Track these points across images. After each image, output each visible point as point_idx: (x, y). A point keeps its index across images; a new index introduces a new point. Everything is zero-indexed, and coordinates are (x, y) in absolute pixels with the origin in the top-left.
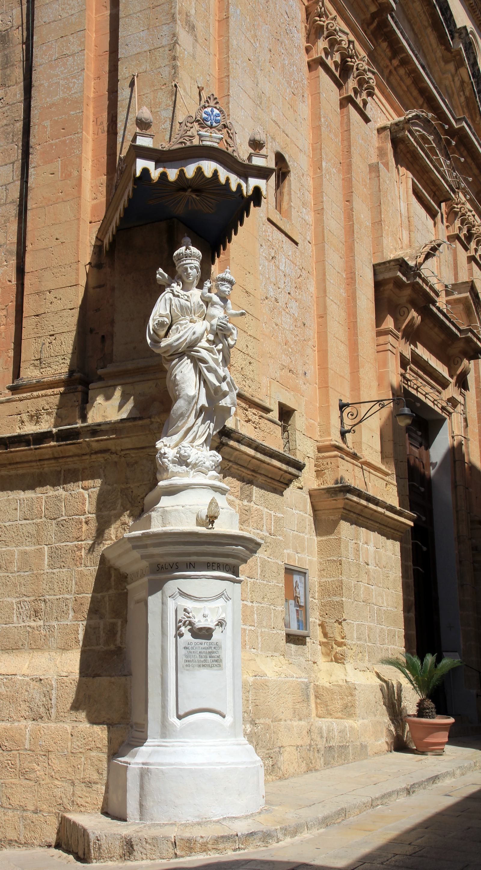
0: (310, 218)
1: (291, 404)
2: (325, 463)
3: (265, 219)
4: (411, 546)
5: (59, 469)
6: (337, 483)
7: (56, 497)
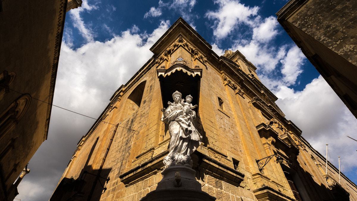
1: (237, 158)
2: (256, 180)
6: (262, 186)
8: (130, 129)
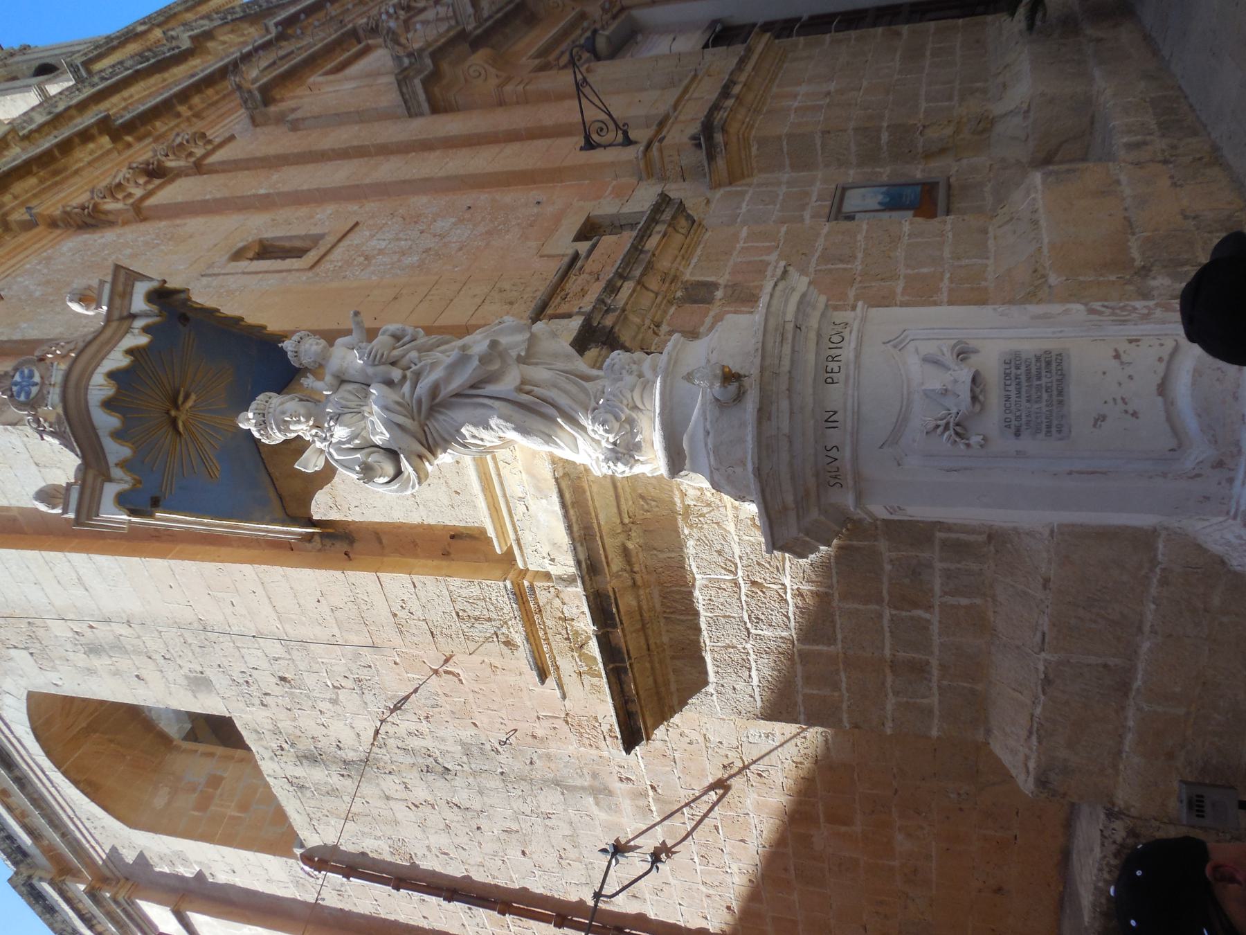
0: (330, 209)
3: (310, 274)
4: (802, 39)
8: (361, 767)
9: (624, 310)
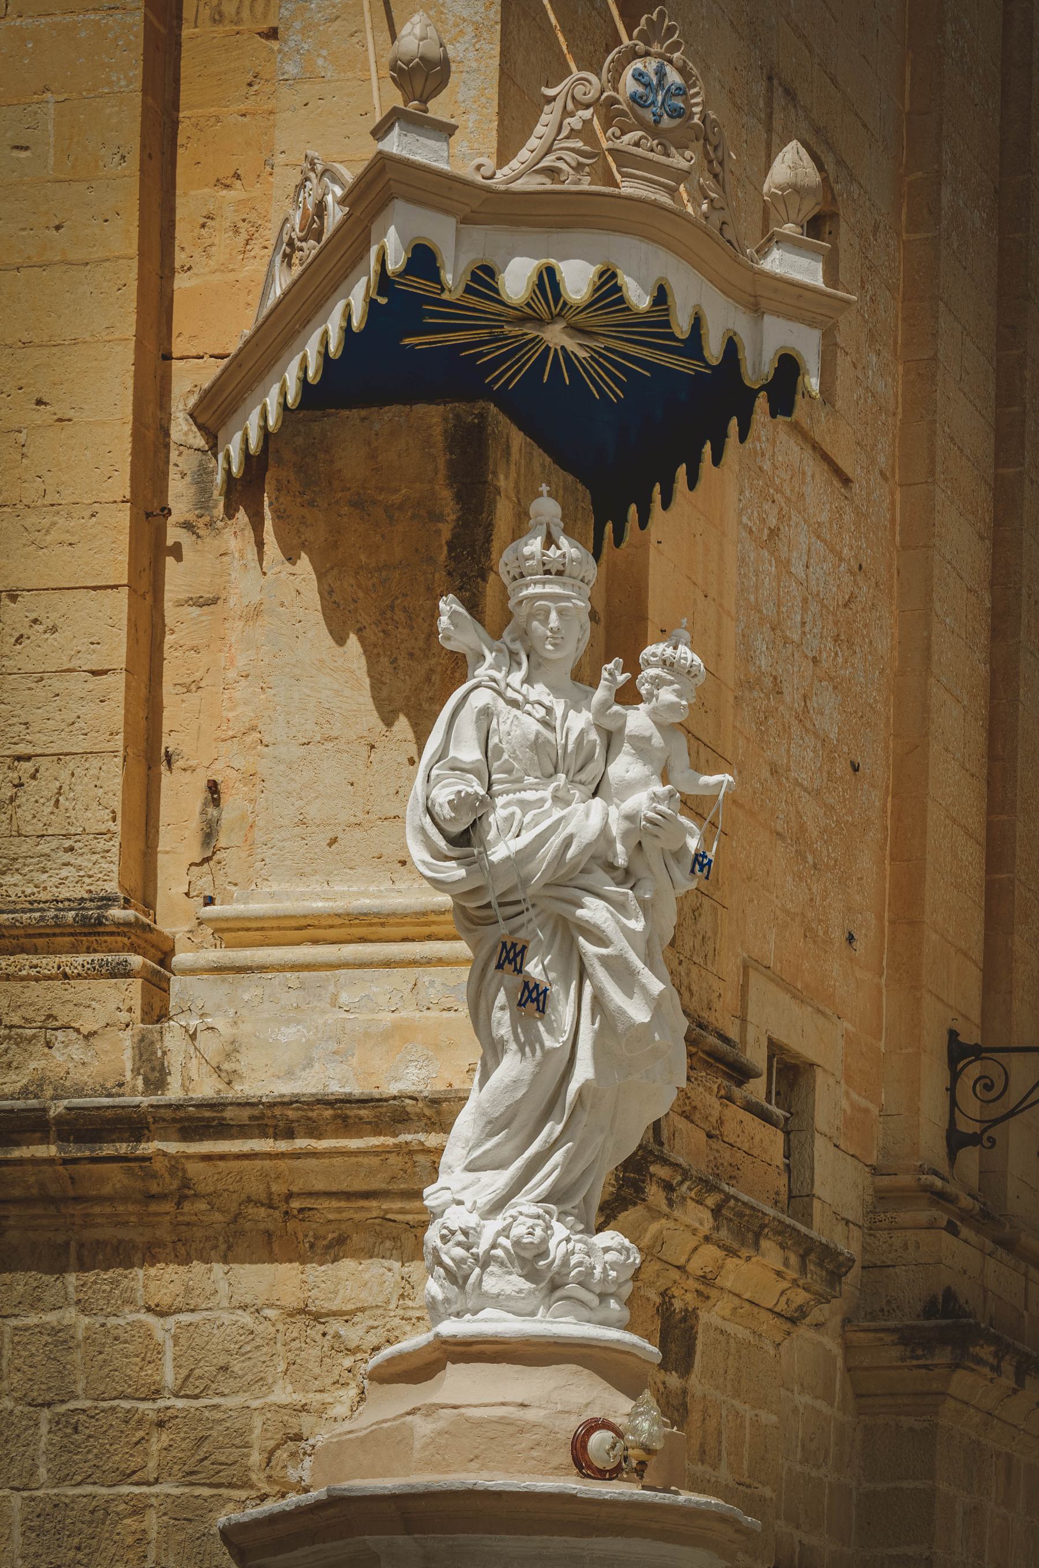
5: (61, 1238)
7: (54, 1331)
9: (667, 1217)
